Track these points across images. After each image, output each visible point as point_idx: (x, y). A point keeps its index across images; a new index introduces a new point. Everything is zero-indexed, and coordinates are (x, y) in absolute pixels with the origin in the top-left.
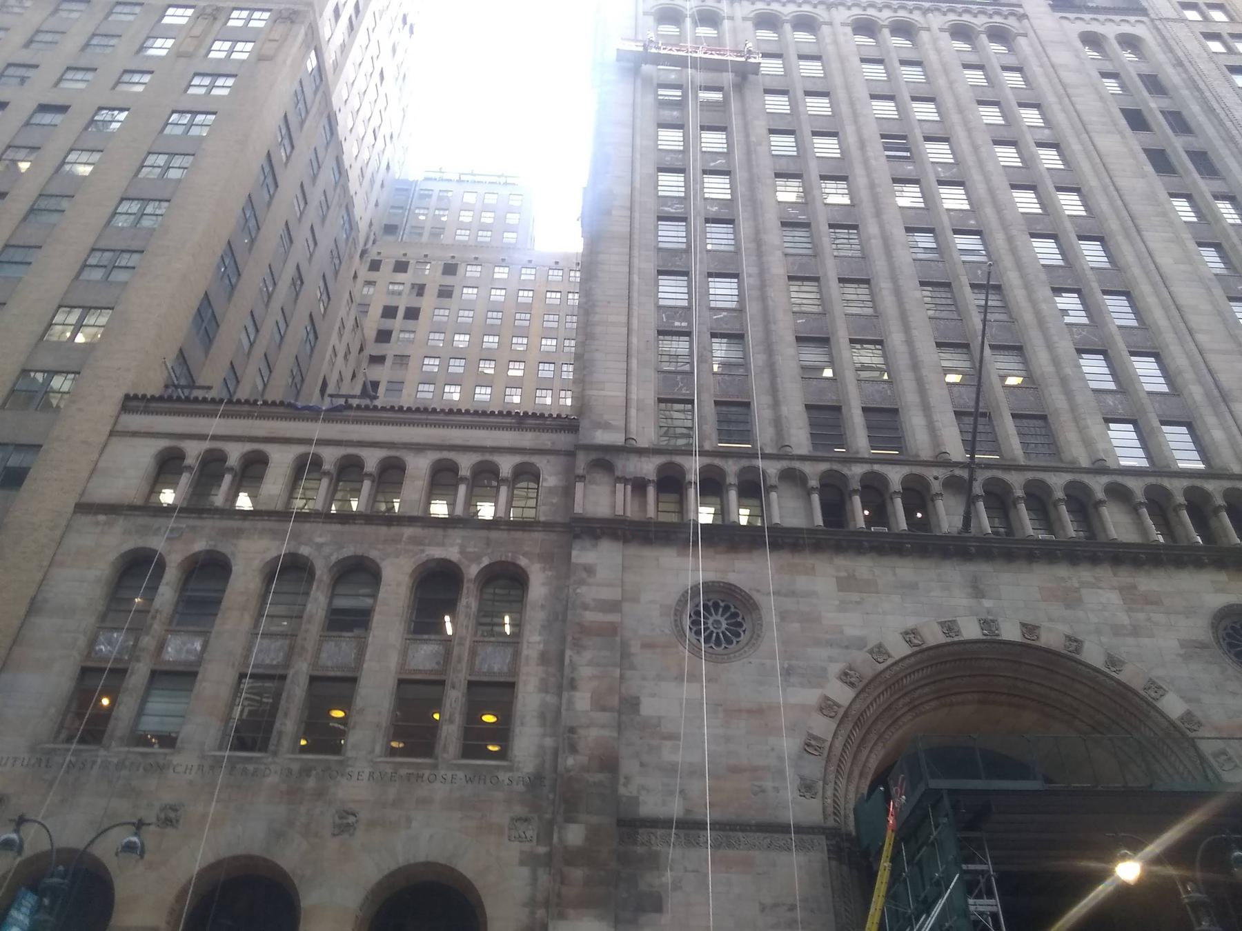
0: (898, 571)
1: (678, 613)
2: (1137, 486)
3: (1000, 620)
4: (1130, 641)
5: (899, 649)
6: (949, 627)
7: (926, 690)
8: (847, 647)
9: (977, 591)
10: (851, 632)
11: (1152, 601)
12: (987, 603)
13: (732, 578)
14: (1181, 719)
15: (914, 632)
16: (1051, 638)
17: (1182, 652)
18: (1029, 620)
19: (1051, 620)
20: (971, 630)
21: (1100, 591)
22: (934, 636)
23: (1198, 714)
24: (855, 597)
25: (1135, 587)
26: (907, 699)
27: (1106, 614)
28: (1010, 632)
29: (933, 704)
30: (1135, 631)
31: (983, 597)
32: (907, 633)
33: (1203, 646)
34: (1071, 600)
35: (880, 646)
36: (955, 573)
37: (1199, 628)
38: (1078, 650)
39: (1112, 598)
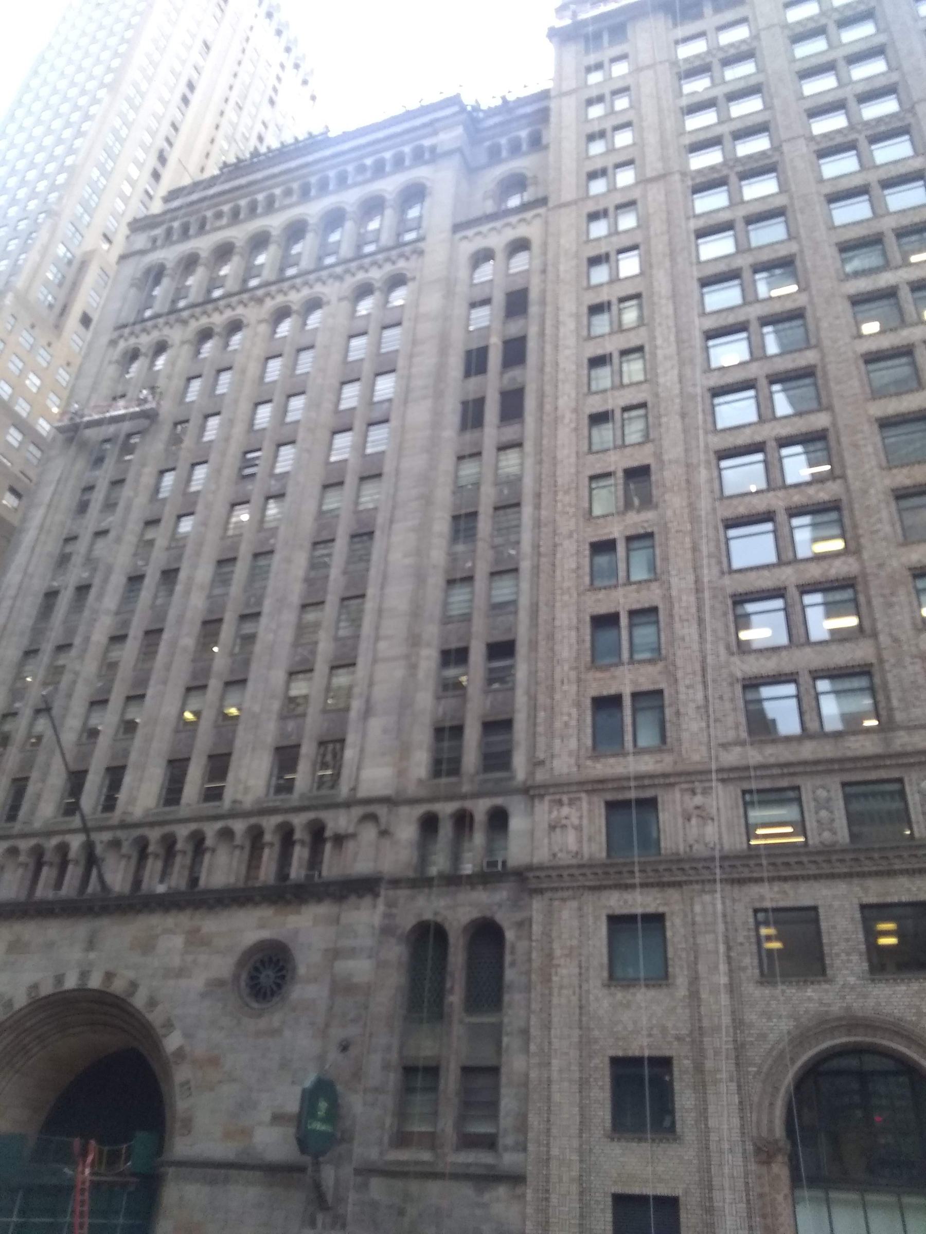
2: (239, 826)
5: (21, 1000)
6: (59, 979)
9: (91, 944)
12: (92, 955)
14: (174, 1054)
15: (35, 987)
16: (118, 986)
20: (71, 983)
22: (47, 989)
23: (188, 1049)
25: (198, 930)
28: (95, 982)
30: (181, 972)
34: (147, 946)
36: (82, 928)
37: (222, 966)
38: (132, 994)
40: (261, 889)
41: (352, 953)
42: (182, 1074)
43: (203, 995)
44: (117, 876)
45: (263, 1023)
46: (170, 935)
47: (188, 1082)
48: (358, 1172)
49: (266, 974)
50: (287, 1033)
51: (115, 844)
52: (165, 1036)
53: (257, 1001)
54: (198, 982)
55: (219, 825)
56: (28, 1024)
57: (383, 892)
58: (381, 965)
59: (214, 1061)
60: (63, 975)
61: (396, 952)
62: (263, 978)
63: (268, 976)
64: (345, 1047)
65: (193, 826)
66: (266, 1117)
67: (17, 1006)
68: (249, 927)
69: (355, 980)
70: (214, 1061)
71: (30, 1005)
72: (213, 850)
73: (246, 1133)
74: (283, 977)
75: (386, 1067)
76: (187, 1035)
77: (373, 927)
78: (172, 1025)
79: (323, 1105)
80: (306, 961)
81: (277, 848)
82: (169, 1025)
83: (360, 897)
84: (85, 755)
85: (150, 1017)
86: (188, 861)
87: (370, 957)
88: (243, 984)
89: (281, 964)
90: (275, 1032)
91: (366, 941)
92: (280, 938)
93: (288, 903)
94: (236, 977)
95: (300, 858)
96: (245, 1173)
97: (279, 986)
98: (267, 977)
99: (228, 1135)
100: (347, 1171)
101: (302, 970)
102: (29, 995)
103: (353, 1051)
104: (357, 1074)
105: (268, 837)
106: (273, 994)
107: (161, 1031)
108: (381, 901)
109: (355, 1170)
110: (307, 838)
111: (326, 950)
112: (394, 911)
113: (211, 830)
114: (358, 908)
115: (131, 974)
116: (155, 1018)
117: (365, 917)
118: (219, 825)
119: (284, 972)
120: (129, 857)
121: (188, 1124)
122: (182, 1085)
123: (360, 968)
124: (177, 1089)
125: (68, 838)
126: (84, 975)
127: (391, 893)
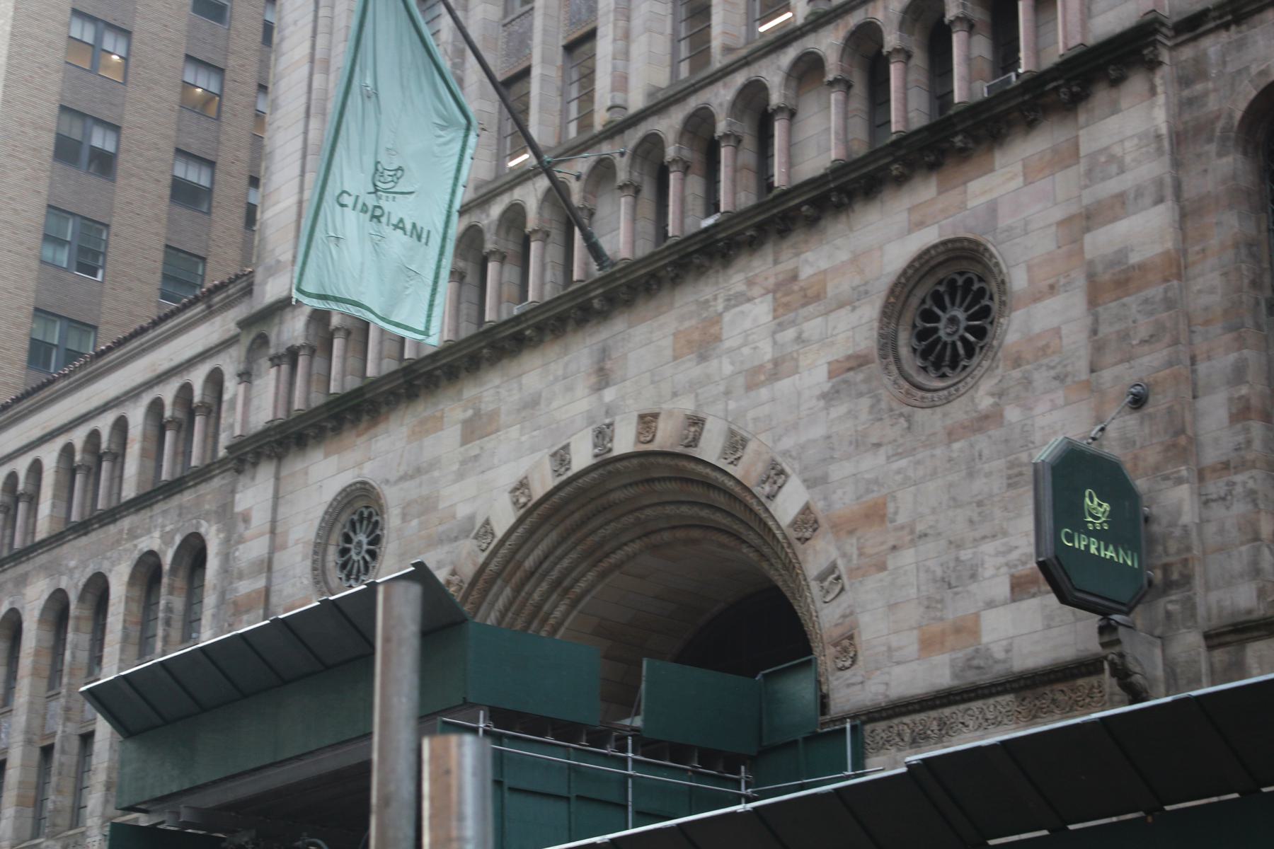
0: (526, 380)
1: (319, 549)
3: (618, 418)
4: (764, 393)
5: (504, 518)
6: (561, 457)
7: (565, 563)
8: (456, 539)
9: (603, 377)
10: (463, 511)
11: (813, 296)
12: (609, 395)
13: (369, 472)
14: (794, 524)
15: (522, 485)
16: (666, 437)
17: (827, 387)
18: (647, 407)
19: (675, 394)
20: (582, 457)
21: (746, 307)
22: (543, 483)
23: (819, 506)
24: (473, 448)
25: (794, 277)
26: (545, 586)
27: (746, 351)
28: (624, 443)
29: (591, 576)
30: (778, 368)
31: (607, 385)
32: (516, 489)
33: (858, 362)
34: (703, 344)
35: (487, 522)
37: (856, 327)
39: (761, 311)
40: (894, 144)
41: (1119, 206)
42: (817, 557)
43: (829, 397)
44: (620, 232)
45: (958, 411)
46: (741, 307)
47: (833, 568)
48: (1213, 639)
49: (947, 314)
50: (1012, 414)
51: (603, 170)
52: (771, 497)
53: (944, 376)
54: (814, 375)
55: (788, 56)
56: (529, 563)
57: (1165, 56)
58: (1188, 214)
59: (875, 514)
60: (566, 448)
61: (1223, 168)
62: (944, 330)
63: (953, 320)
64: (1138, 402)
65: (740, 79)
66: (1002, 588)
67: (500, 532)
68: (890, 236)
69: (1134, 259)
70: (875, 514)
71: (520, 521)
72: (792, 114)
73: (967, 629)
74: (985, 312)
75: (1241, 413)
76: (810, 483)
77: (1158, 137)
78: (782, 472)
79: (1097, 508)
80: (1021, 259)
81: (919, 59)
82: (776, 474)
83: (1116, 82)
84: (521, 43)
85: (736, 471)
86: (748, 155)
87: (1160, 200)
88: (904, 351)
89: (976, 286)
90: (984, 421)
91: (1149, 169)
92: (961, 234)
93: (963, 155)
94: (888, 344)
95: (969, 60)
96: (976, 705)
97: (980, 333)
98: (953, 323)
99: (929, 644)
100: (1189, 642)
101: (1018, 280)
102: (516, 503)
103: (1158, 403)
104: (1180, 445)
105: (891, 40)
106: (970, 352)
107: (762, 491)
108: (1161, 77)
109: (1207, 636)
110: (978, 14)
111: (1061, 223)
112: (1199, 87)
113: (773, 72)
114: (1115, 110)
115: (687, 405)
116: (747, 469)
117: (1130, 124)
118: (788, 56)
119: (985, 302)
120: (637, 191)
121: (847, 645)
122: (822, 578)
123: (1144, 232)
124: (814, 586)
125: (517, 194)
126: (603, 435)
127: (1187, 53)
